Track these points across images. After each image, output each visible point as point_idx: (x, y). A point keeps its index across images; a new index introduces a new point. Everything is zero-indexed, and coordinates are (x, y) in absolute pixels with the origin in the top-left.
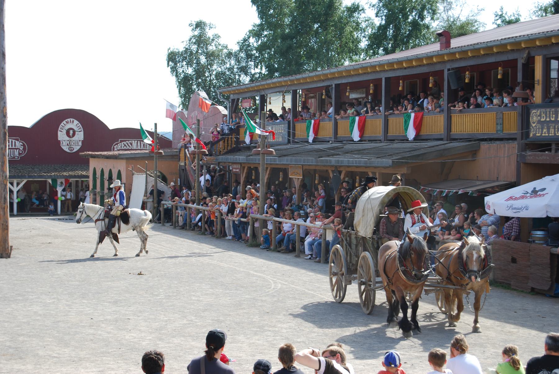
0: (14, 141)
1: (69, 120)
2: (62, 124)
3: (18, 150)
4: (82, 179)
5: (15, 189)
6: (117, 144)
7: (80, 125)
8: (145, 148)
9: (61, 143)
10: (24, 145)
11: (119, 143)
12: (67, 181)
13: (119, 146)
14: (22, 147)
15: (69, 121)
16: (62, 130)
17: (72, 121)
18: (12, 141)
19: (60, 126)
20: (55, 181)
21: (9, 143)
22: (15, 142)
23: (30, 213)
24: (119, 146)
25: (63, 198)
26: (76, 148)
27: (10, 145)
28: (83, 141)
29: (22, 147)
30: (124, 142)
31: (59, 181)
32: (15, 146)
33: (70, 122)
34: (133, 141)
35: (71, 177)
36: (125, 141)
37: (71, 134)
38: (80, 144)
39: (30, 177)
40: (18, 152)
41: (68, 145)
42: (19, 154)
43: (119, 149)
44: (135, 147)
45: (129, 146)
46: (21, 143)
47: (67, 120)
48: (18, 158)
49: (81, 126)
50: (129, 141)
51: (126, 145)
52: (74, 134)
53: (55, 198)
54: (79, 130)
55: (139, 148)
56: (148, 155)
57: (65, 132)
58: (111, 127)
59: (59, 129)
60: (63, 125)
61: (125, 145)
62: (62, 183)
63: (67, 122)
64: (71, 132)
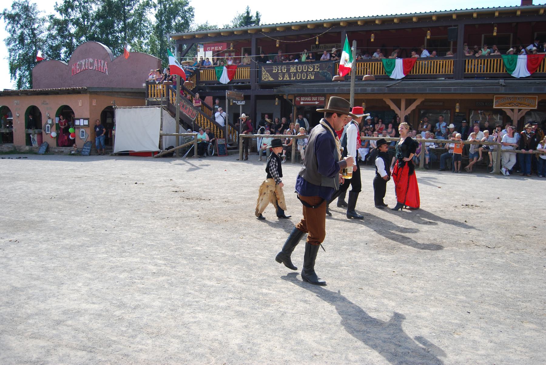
56: (111, 91)
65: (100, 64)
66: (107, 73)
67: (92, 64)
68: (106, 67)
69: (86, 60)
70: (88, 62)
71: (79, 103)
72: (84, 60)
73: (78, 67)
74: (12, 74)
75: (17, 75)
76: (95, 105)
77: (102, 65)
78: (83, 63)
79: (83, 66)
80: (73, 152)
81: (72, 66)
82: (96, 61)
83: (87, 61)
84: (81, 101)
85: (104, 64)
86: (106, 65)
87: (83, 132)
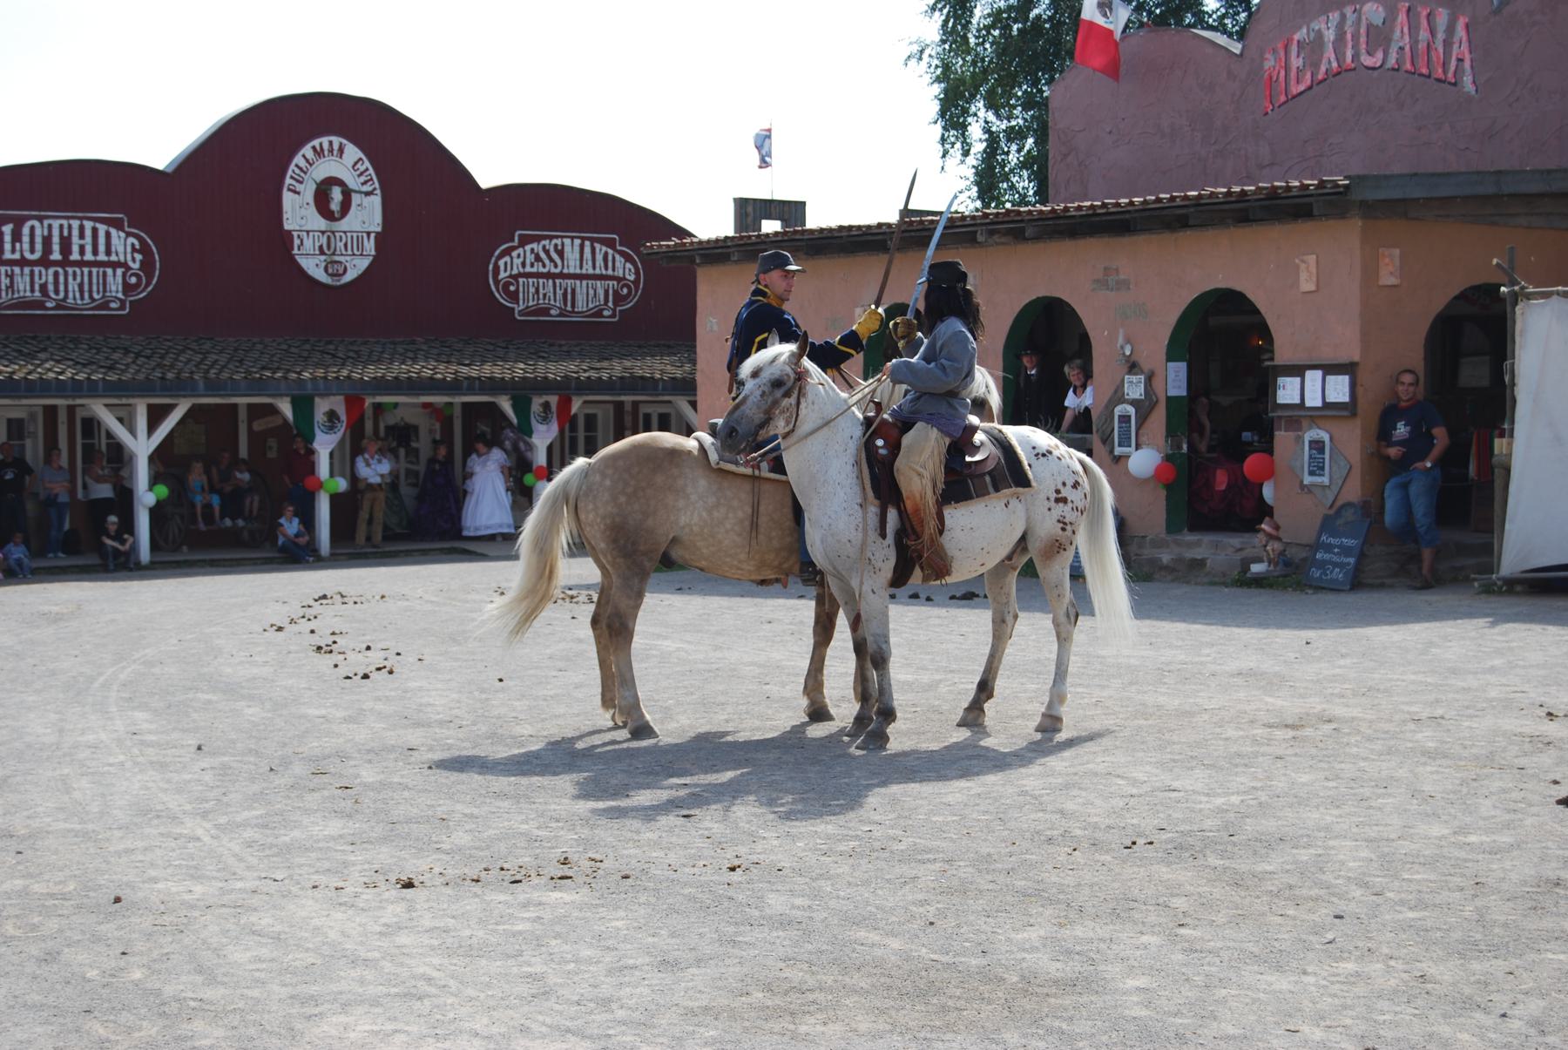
0: (102, 228)
1: (325, 140)
2: (298, 160)
3: (120, 271)
4: (379, 399)
5: (142, 446)
6: (507, 252)
7: (367, 164)
8: (610, 272)
9: (297, 242)
10: (144, 250)
11: (514, 248)
12: (353, 403)
13: (517, 262)
14: (138, 257)
15: (326, 146)
16: (299, 187)
17: (336, 147)
18: (95, 231)
19: (292, 167)
20: (303, 405)
21: (82, 236)
22: (108, 235)
23: (185, 554)
24: (517, 262)
25: (341, 484)
26: (356, 267)
27: (89, 248)
28: (381, 239)
29: (138, 257)
30: (534, 246)
31: (322, 407)
32: (108, 253)
33: (331, 151)
34: (567, 241)
35: (381, 385)
36: (538, 239)
37: (335, 206)
38: (370, 246)
39: (213, 387)
40: (119, 279)
41: (322, 252)
42: (127, 288)
43: (515, 272)
44: (573, 268)
45: (551, 260)
46: (131, 240)
47: (316, 143)
48: (122, 307)
49: (371, 171)
50: (551, 238)
51: (543, 255)
52: (346, 206)
53: (309, 482)
54: (367, 188)
55: (588, 269)
57: (308, 191)
58: (485, 180)
59: (288, 181)
60: (303, 163)
61: (538, 258)
62: (332, 416)
63: (319, 153)
64: (336, 194)
65: (1424, 35)
66: (1467, 80)
67: (1378, 37)
68: (1461, 48)
69: (1343, 17)
70: (1359, 19)
71: (1303, 276)
72: (1335, 17)
73: (1296, 62)
74: (945, 128)
75: (975, 131)
76: (1392, 281)
77: (1440, 36)
78: (1330, 35)
79: (1329, 53)
80: (1256, 568)
81: (1263, 59)
82: (1402, 17)
83: (1351, 17)
84: (1312, 259)
85: (1450, 30)
86: (1460, 32)
87: (1317, 446)
